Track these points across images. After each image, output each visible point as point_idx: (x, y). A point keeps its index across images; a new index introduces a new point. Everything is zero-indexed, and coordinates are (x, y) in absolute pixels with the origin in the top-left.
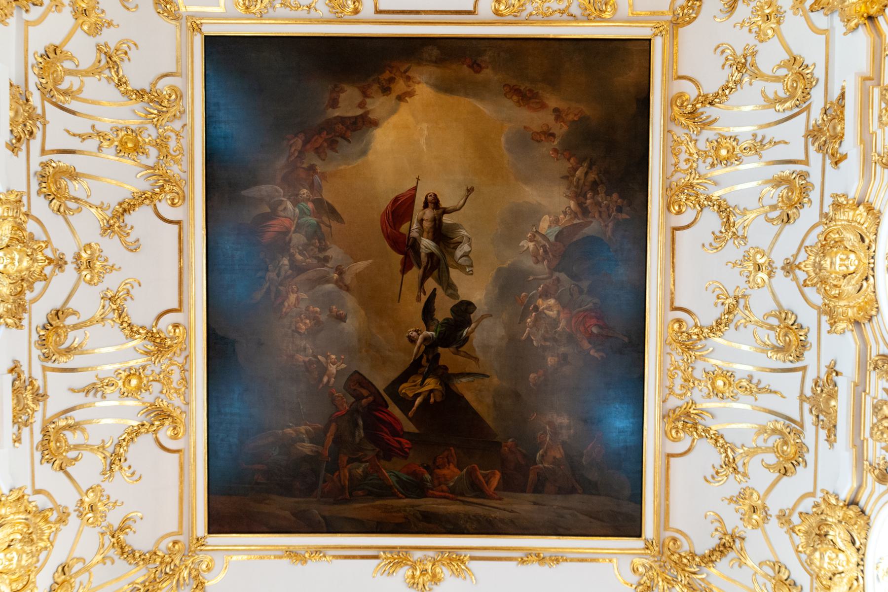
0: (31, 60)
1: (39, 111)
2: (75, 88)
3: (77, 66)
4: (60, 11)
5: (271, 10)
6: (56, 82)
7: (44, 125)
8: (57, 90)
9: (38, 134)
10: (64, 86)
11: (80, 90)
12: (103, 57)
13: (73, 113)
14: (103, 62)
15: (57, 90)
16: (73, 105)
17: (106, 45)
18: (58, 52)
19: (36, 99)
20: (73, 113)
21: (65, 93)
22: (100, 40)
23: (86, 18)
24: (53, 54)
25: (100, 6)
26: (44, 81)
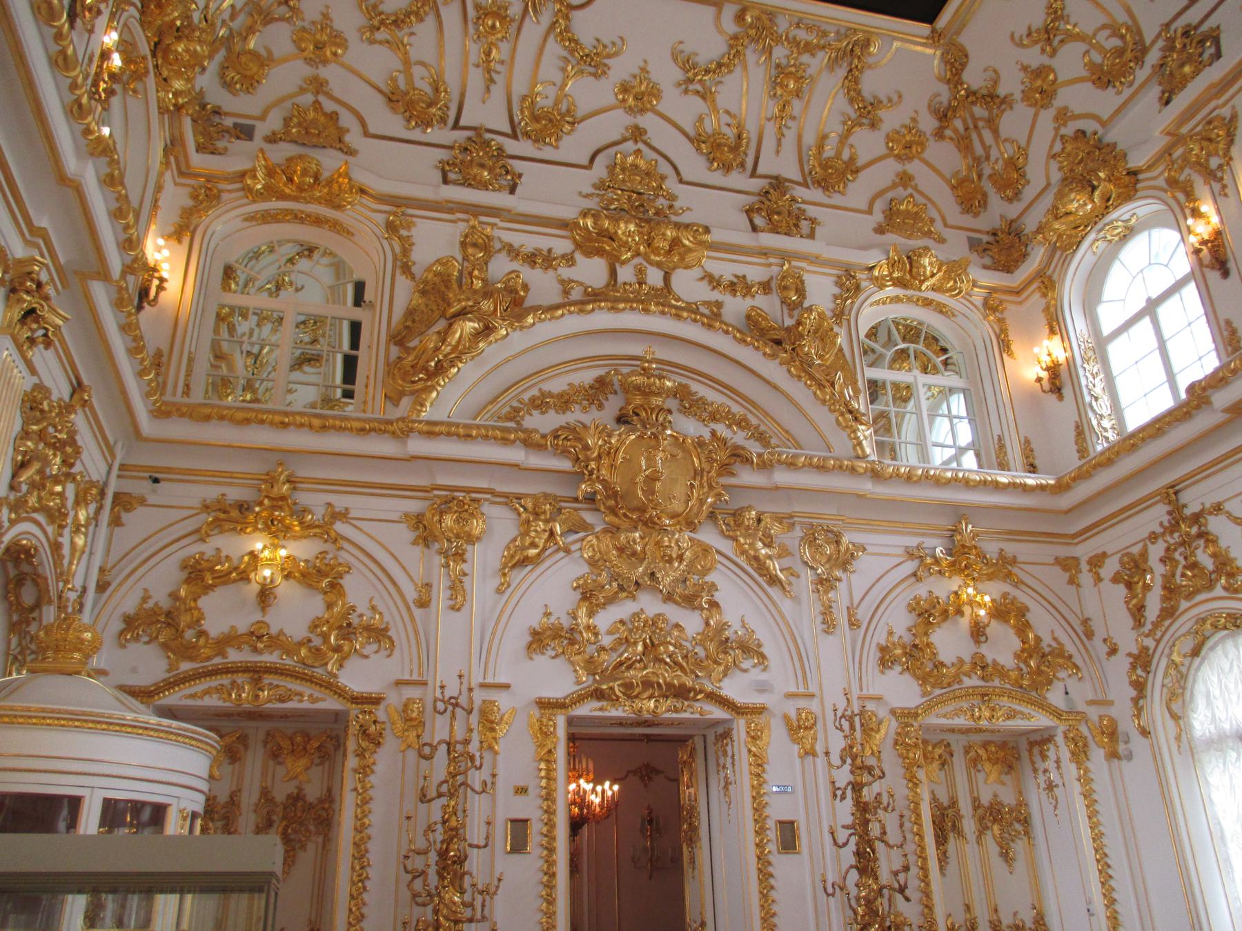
0: (1127, 92)
1: (1161, 43)
2: (1107, 32)
3: (1087, 52)
4: (1066, 108)
5: (843, 31)
6: (1120, 52)
7: (1168, 25)
8: (1125, 43)
9: (1180, 23)
10: (1116, 42)
11: (1104, 27)
12: (1055, 43)
13: (1129, 12)
14: (1058, 38)
15: (1125, 43)
16: (1122, 17)
17: (1043, 51)
18: (1095, 77)
19: (1153, 57)
20: (1129, 12)
21: (1122, 37)
22: (1045, 60)
23: (1045, 87)
24: (1103, 78)
25: (1023, 87)
26: (1132, 64)
